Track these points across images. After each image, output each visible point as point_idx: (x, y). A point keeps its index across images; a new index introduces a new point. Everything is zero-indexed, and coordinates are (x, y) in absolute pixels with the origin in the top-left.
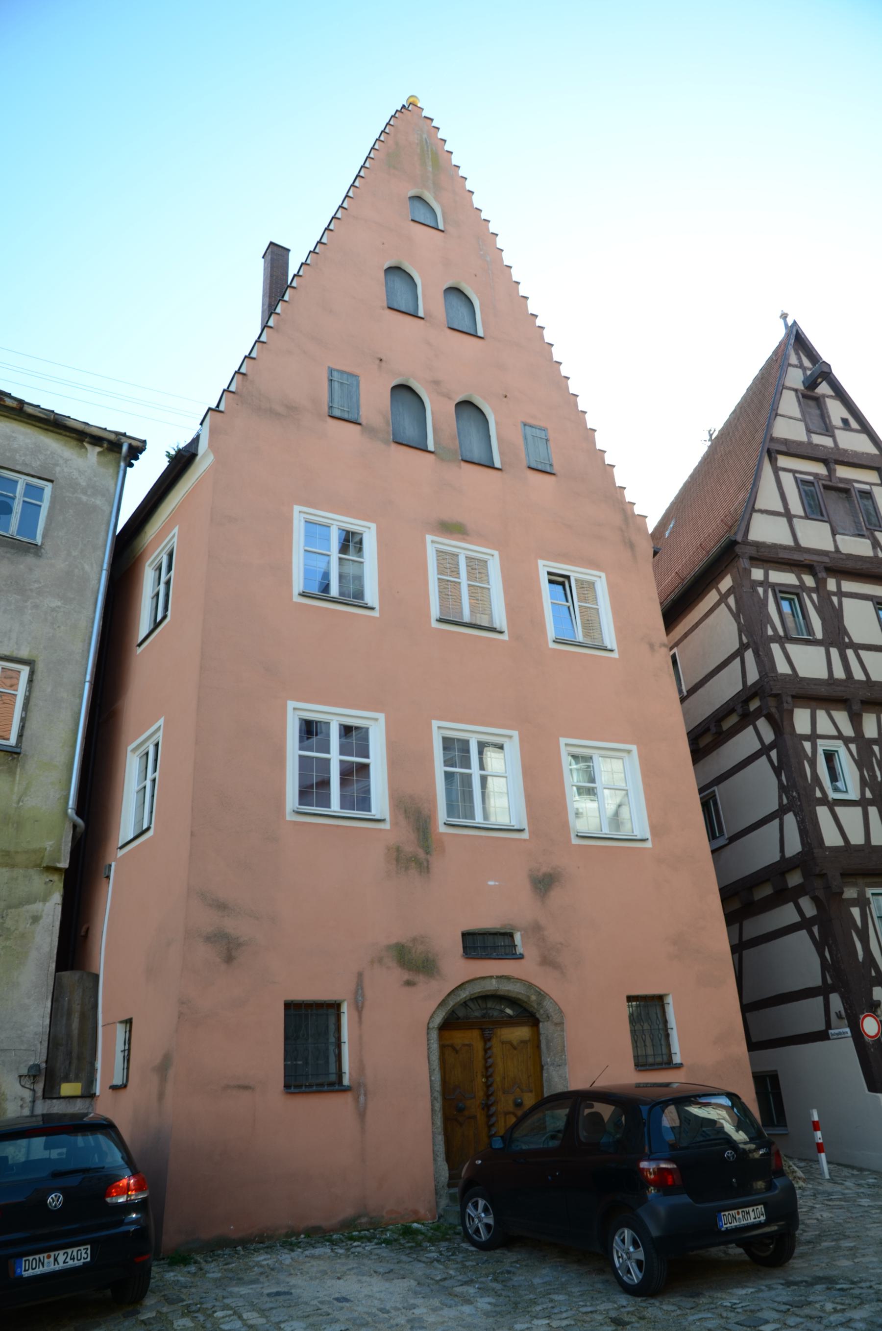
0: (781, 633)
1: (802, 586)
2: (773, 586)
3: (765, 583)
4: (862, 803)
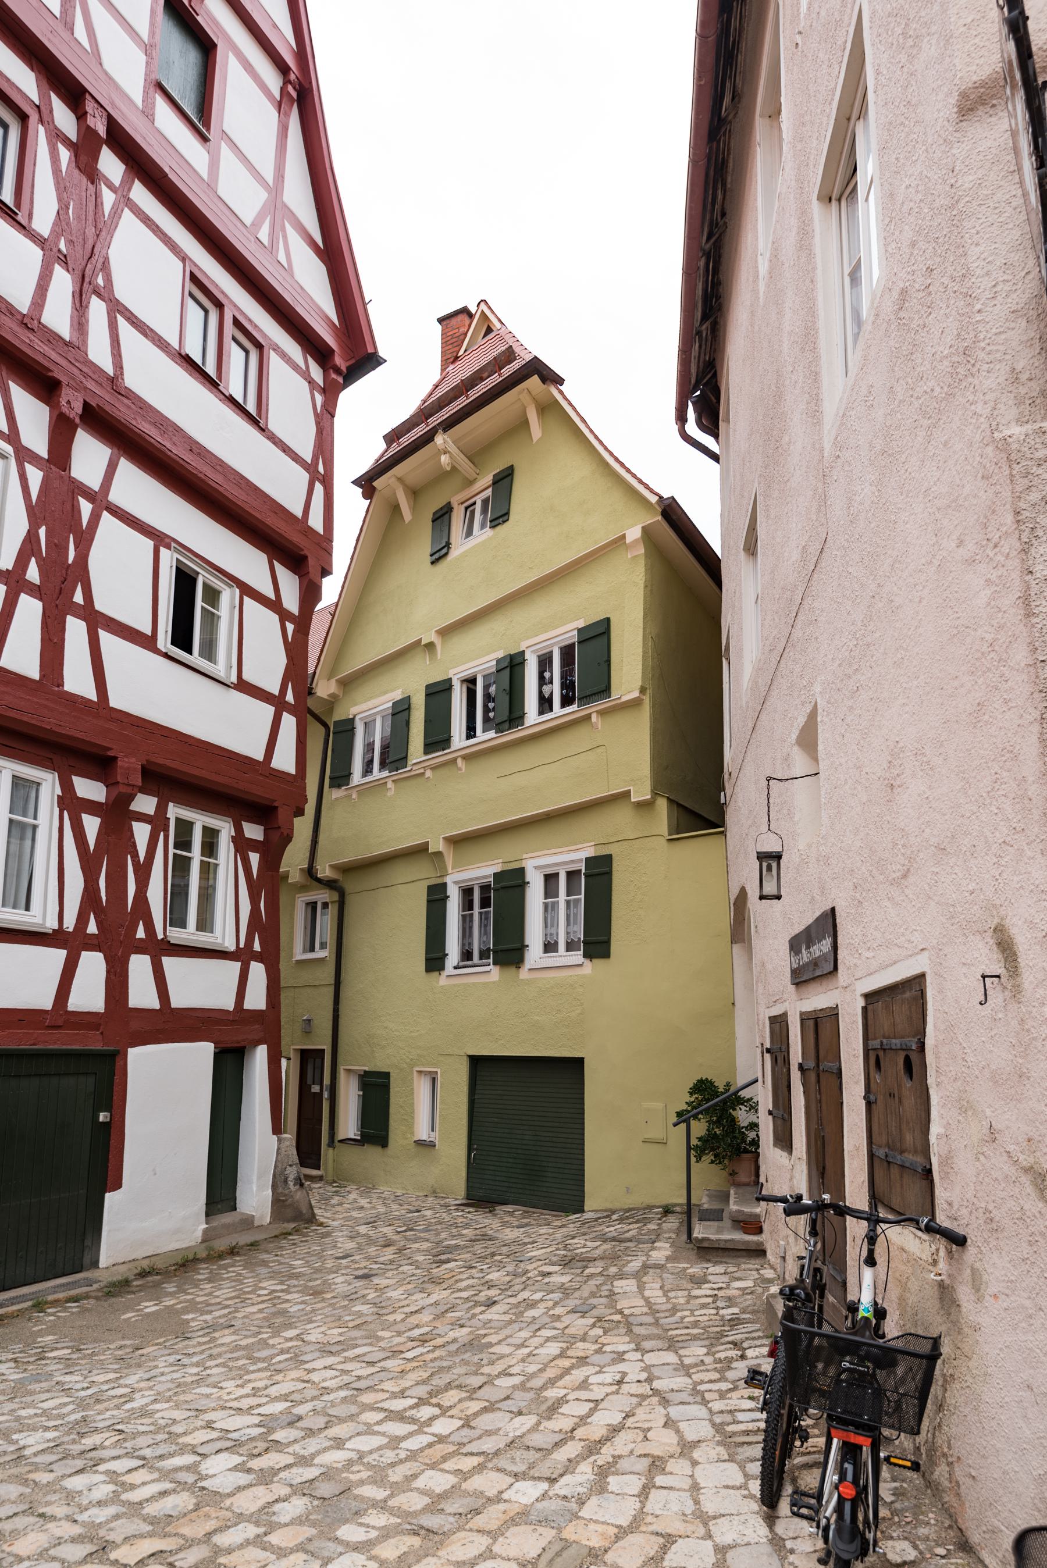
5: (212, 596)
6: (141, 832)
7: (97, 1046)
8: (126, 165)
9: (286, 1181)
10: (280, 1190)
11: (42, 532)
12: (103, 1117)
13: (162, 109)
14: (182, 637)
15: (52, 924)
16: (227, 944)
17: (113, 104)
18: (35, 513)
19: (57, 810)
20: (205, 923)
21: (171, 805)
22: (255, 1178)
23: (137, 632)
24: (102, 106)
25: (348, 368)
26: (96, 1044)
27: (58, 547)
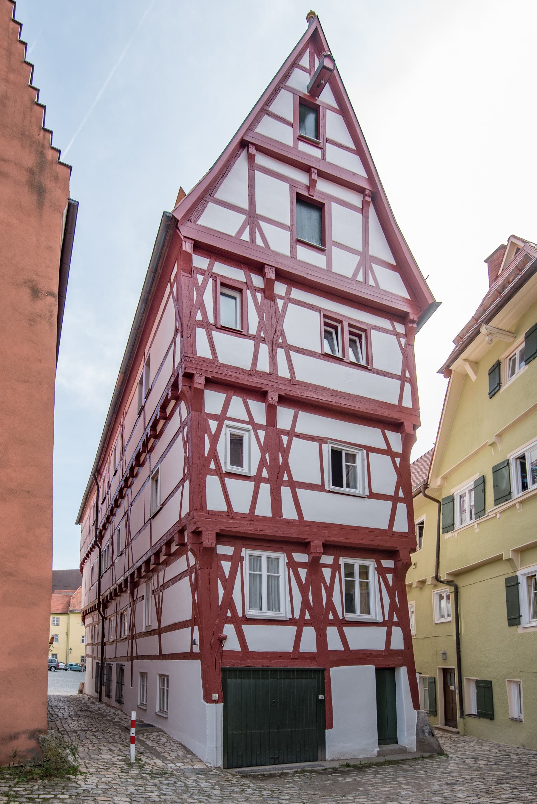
0: (211, 320)
1: (248, 284)
2: (215, 277)
3: (209, 273)
4: (258, 480)
5: (352, 457)
6: (327, 573)
7: (316, 667)
8: (287, 284)
9: (424, 732)
10: (421, 737)
11: (267, 456)
12: (321, 697)
13: (301, 251)
14: (337, 481)
15: (289, 616)
16: (378, 619)
17: (277, 262)
18: (263, 449)
19: (287, 569)
20: (366, 609)
21: (341, 558)
22: (405, 730)
23: (315, 485)
24: (272, 266)
25: (418, 318)
26: (314, 666)
27: (274, 459)
